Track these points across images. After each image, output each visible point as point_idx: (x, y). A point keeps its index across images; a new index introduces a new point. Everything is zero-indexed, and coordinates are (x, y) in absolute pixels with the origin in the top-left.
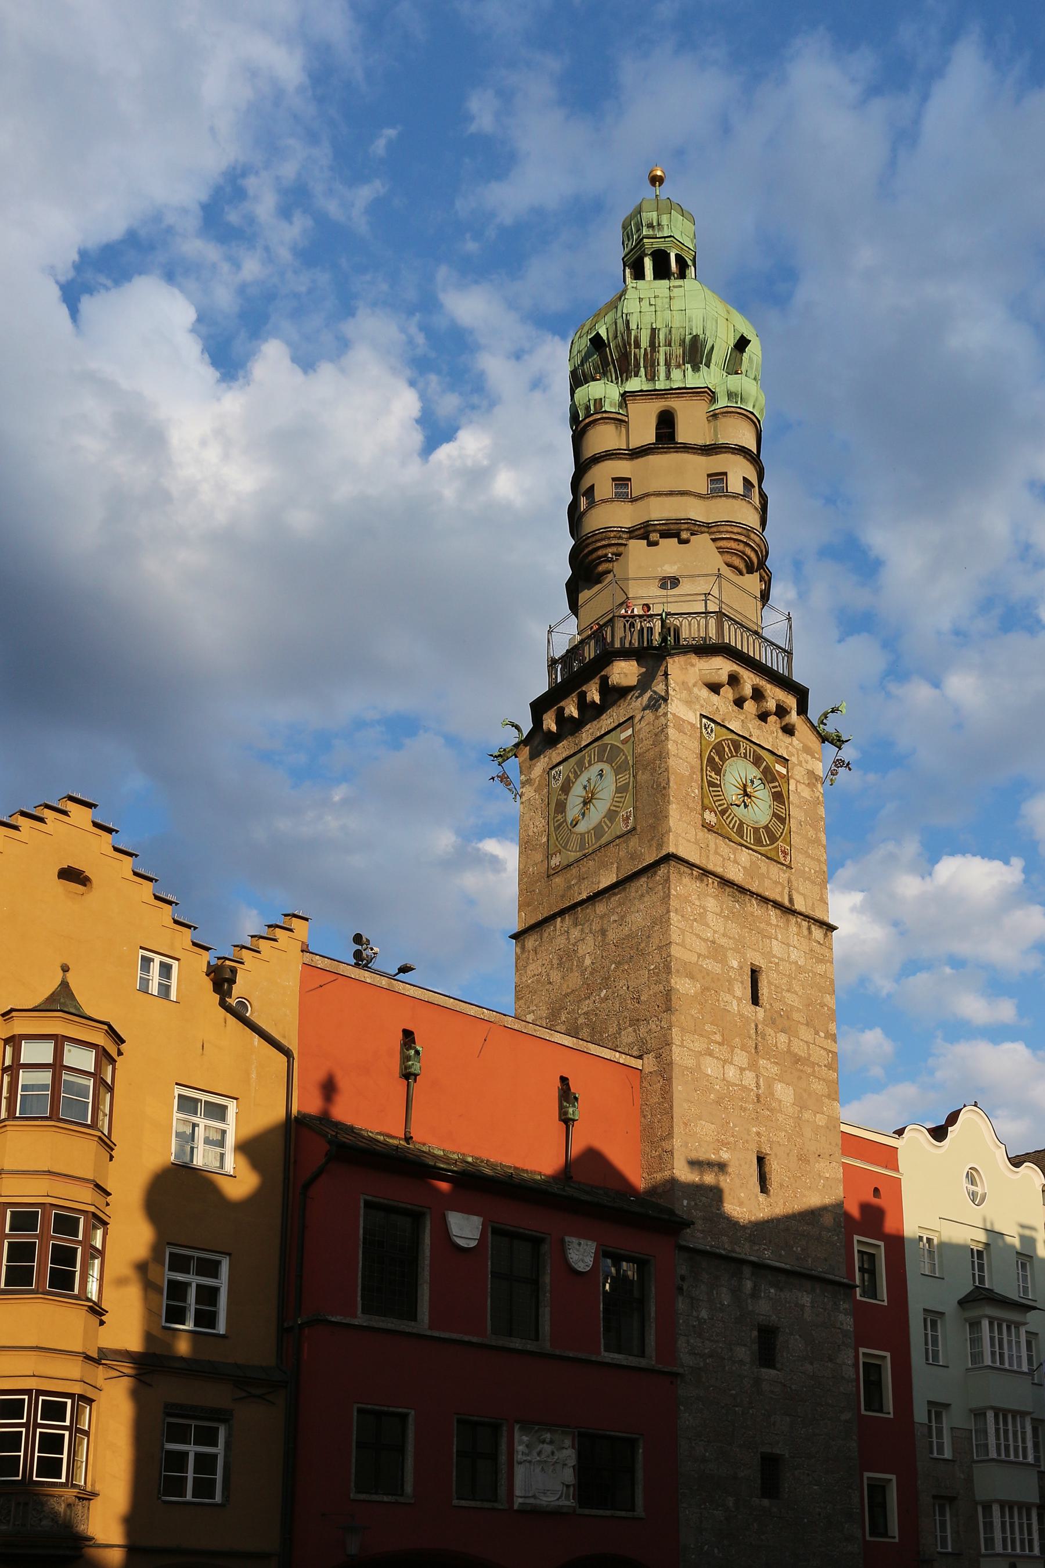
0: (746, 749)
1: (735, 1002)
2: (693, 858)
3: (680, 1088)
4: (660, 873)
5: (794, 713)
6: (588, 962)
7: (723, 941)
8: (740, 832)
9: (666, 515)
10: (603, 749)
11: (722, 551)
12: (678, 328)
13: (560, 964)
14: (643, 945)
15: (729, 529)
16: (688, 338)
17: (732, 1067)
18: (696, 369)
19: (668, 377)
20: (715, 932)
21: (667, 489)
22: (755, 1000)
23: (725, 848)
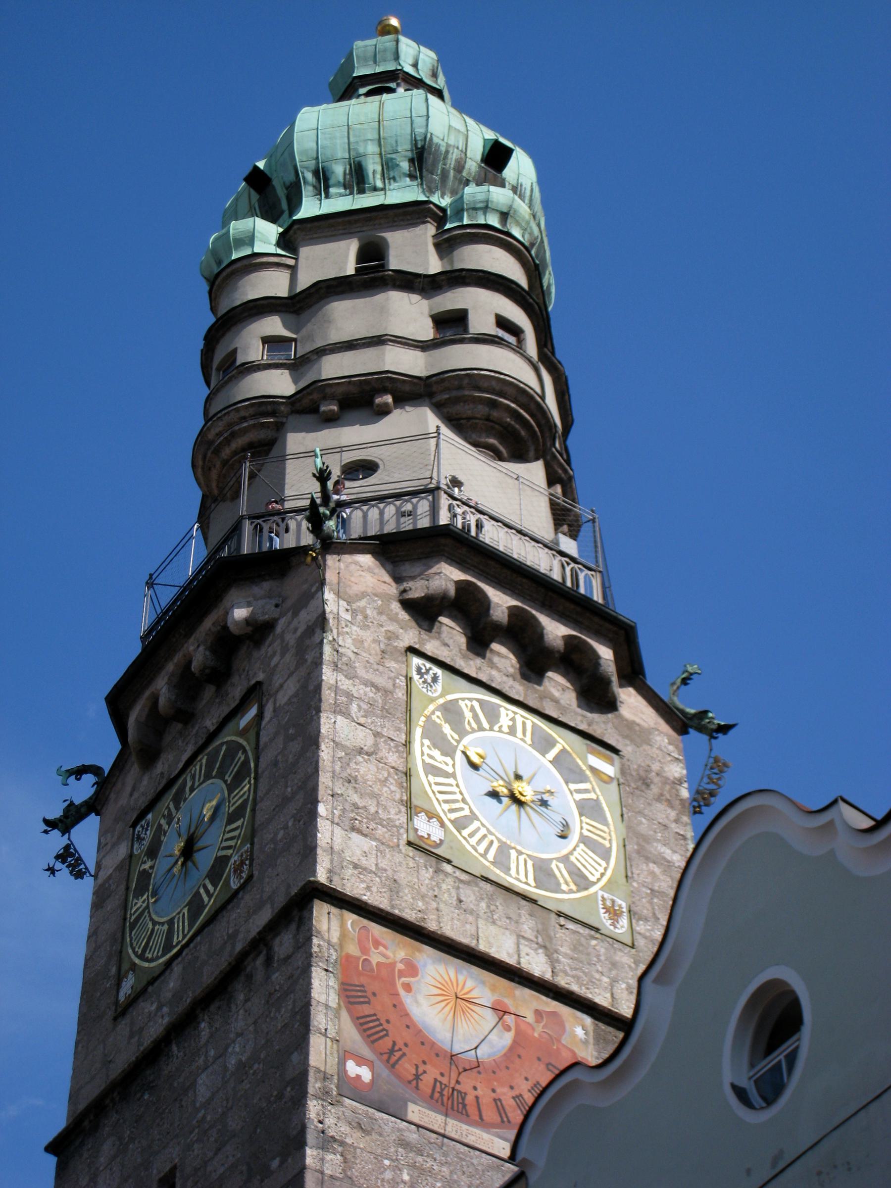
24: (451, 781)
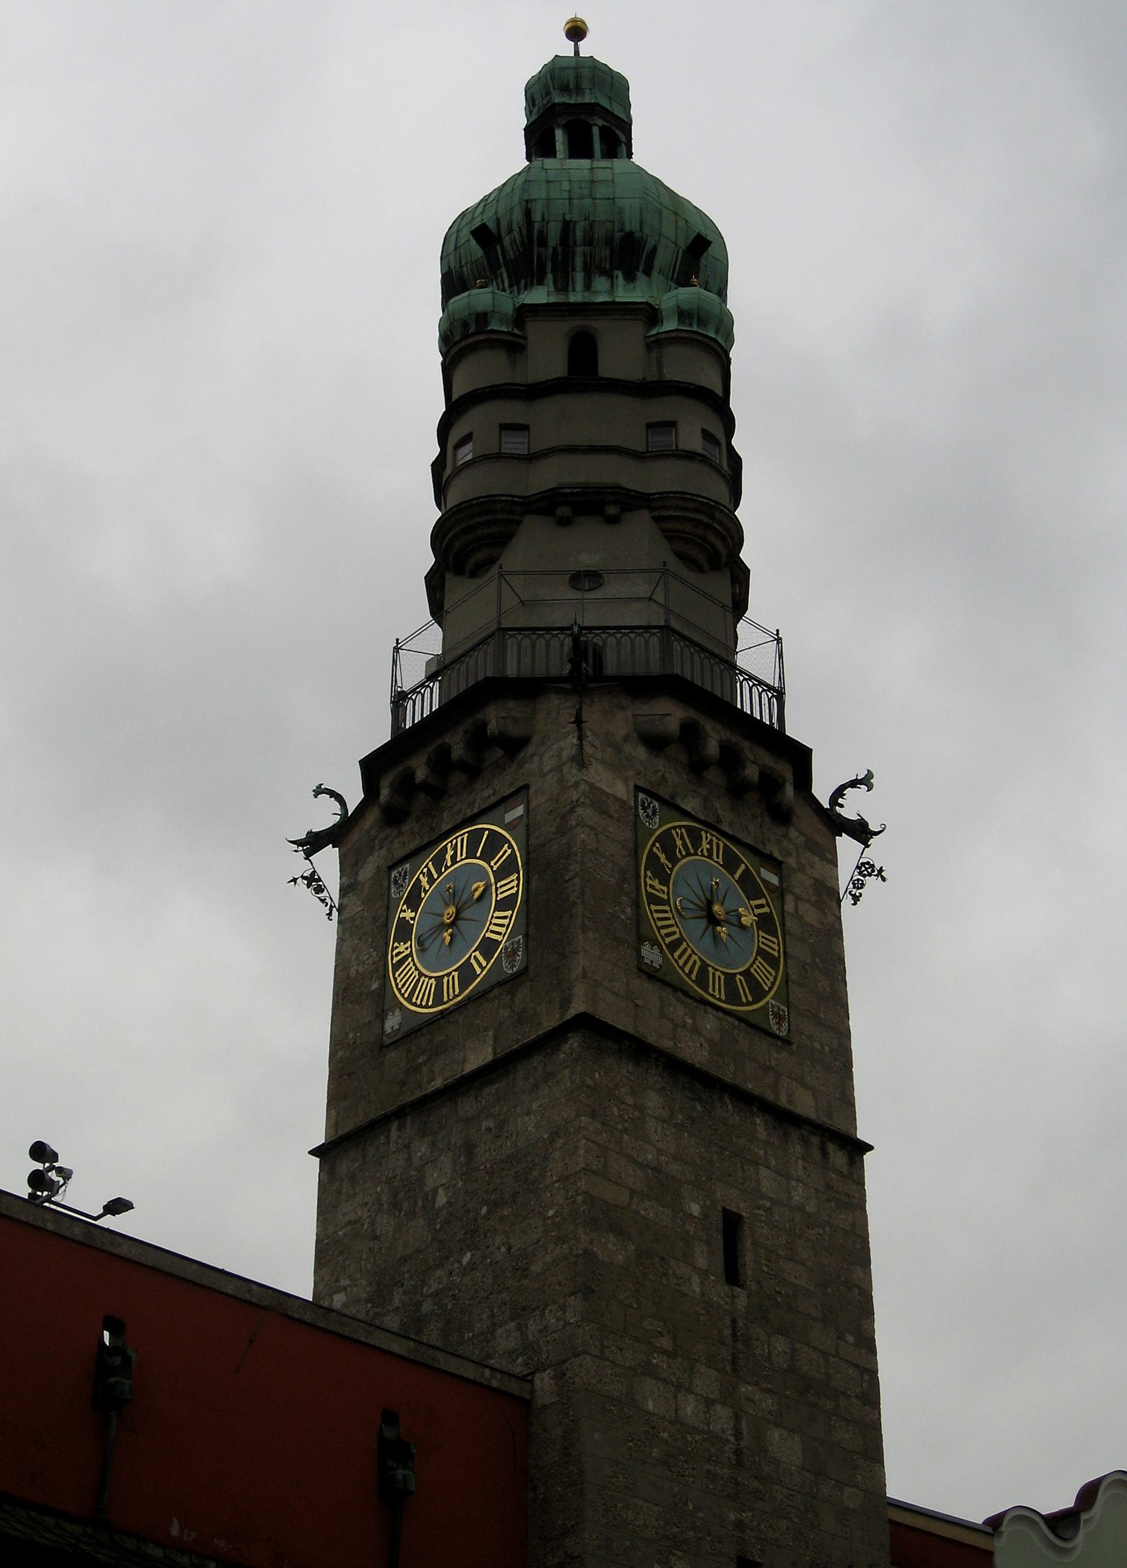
0: (710, 843)
1: (696, 1279)
2: (623, 1022)
3: (596, 1436)
4: (566, 1047)
5: (789, 790)
6: (442, 1199)
7: (675, 1168)
8: (702, 979)
9: (582, 479)
10: (475, 837)
11: (670, 536)
12: (605, 222)
13: (395, 1205)
14: (535, 1173)
15: (682, 504)
16: (618, 235)
17: (691, 1397)
18: (630, 278)
19: (588, 287)
20: (660, 1151)
21: (582, 440)
22: (733, 1275)
23: (678, 1010)
24: (666, 908)
